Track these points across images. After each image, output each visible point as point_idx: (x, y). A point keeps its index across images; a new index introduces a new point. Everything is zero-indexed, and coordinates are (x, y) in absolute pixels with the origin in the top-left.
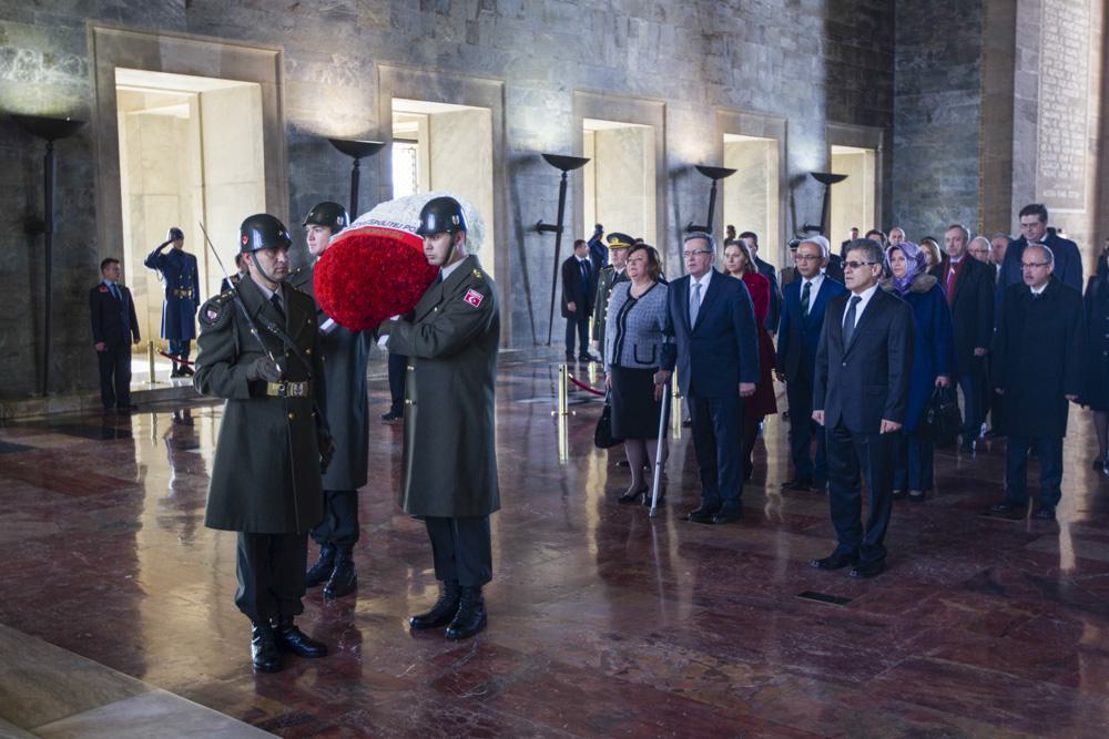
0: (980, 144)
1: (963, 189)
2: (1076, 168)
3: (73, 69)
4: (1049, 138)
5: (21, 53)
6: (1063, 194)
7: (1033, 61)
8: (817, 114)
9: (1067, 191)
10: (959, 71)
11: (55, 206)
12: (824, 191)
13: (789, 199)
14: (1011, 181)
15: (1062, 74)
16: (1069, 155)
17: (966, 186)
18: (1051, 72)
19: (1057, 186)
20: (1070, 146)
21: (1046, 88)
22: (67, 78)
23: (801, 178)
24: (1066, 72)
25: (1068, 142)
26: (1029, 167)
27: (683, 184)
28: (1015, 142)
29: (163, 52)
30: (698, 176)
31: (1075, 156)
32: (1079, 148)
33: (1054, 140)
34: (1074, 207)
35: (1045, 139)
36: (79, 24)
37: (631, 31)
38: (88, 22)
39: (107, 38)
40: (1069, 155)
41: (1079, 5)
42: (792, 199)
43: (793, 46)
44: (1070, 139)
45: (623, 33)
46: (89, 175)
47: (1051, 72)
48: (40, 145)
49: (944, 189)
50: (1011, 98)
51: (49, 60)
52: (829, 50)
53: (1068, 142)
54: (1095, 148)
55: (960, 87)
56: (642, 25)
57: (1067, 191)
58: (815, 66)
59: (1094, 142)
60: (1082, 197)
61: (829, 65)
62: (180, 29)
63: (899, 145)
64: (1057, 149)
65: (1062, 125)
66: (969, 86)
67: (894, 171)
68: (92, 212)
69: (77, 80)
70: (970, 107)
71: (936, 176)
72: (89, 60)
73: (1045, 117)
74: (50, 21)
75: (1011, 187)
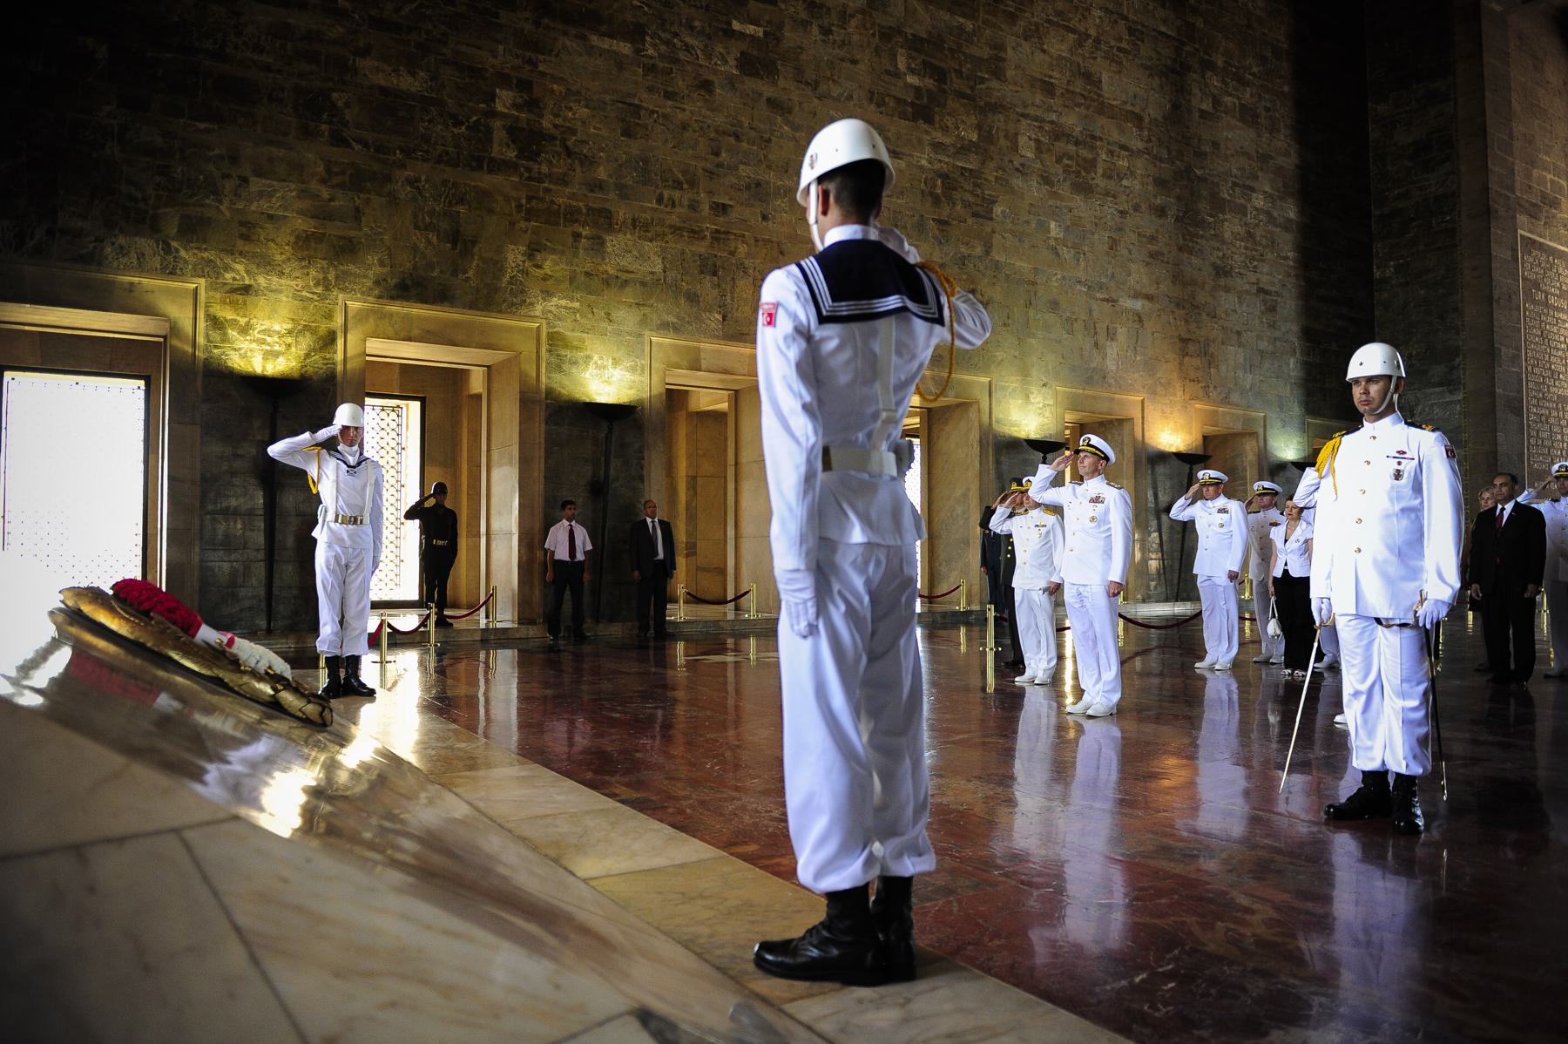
0: (1464, 436)
3: (633, 369)
5: (596, 358)
7: (1516, 359)
8: (1296, 410)
10: (1438, 371)
11: (612, 473)
15: (1549, 373)
18: (1536, 370)
21: (1531, 385)
22: (628, 376)
24: (1553, 372)
27: (1161, 469)
29: (703, 355)
30: (1176, 462)
36: (641, 335)
37: (1111, 335)
38: (647, 333)
39: (660, 345)
41: (1562, 310)
43: (1271, 348)
44: (1562, 434)
45: (1102, 337)
46: (641, 450)
47: (1536, 370)
48: (604, 425)
50: (1493, 394)
51: (616, 362)
52: (1306, 352)
55: (1440, 384)
56: (1122, 332)
58: (1293, 366)
61: (1307, 366)
62: (717, 337)
65: (1552, 421)
66: (1450, 383)
68: (641, 479)
69: (636, 378)
70: (1451, 402)
72: (646, 362)
73: (1531, 412)
74: (619, 333)
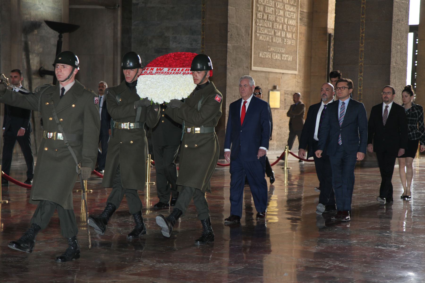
1: (188, 46)
2: (289, 36)
4: (265, 6)
6: (278, 57)
9: (281, 54)
12: (58, 39)
13: (23, 44)
14: (226, 42)
16: (283, 24)
17: (191, 44)
19: (272, 49)
20: (284, 17)
23: (35, 25)
25: (282, 13)
26: (243, 30)
28: (229, 7)
31: (288, 25)
32: (291, 18)
33: (269, 10)
34: (287, 68)
35: (261, 8)
40: (283, 24)
42: (26, 44)
44: (284, 10)
49: (173, 45)
53: (282, 13)
54: (305, 20)
57: (281, 54)
59: (305, 15)
60: (294, 60)
63: (137, 4)
64: (272, 18)
67: (133, 27)
71: (166, 34)
75: (226, 46)
